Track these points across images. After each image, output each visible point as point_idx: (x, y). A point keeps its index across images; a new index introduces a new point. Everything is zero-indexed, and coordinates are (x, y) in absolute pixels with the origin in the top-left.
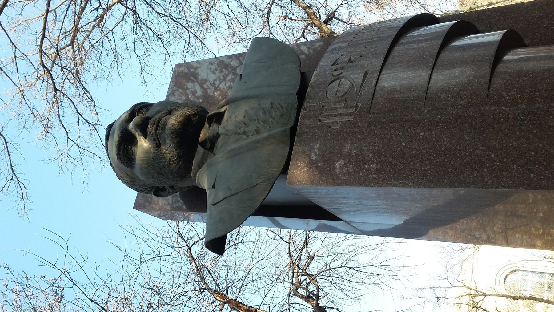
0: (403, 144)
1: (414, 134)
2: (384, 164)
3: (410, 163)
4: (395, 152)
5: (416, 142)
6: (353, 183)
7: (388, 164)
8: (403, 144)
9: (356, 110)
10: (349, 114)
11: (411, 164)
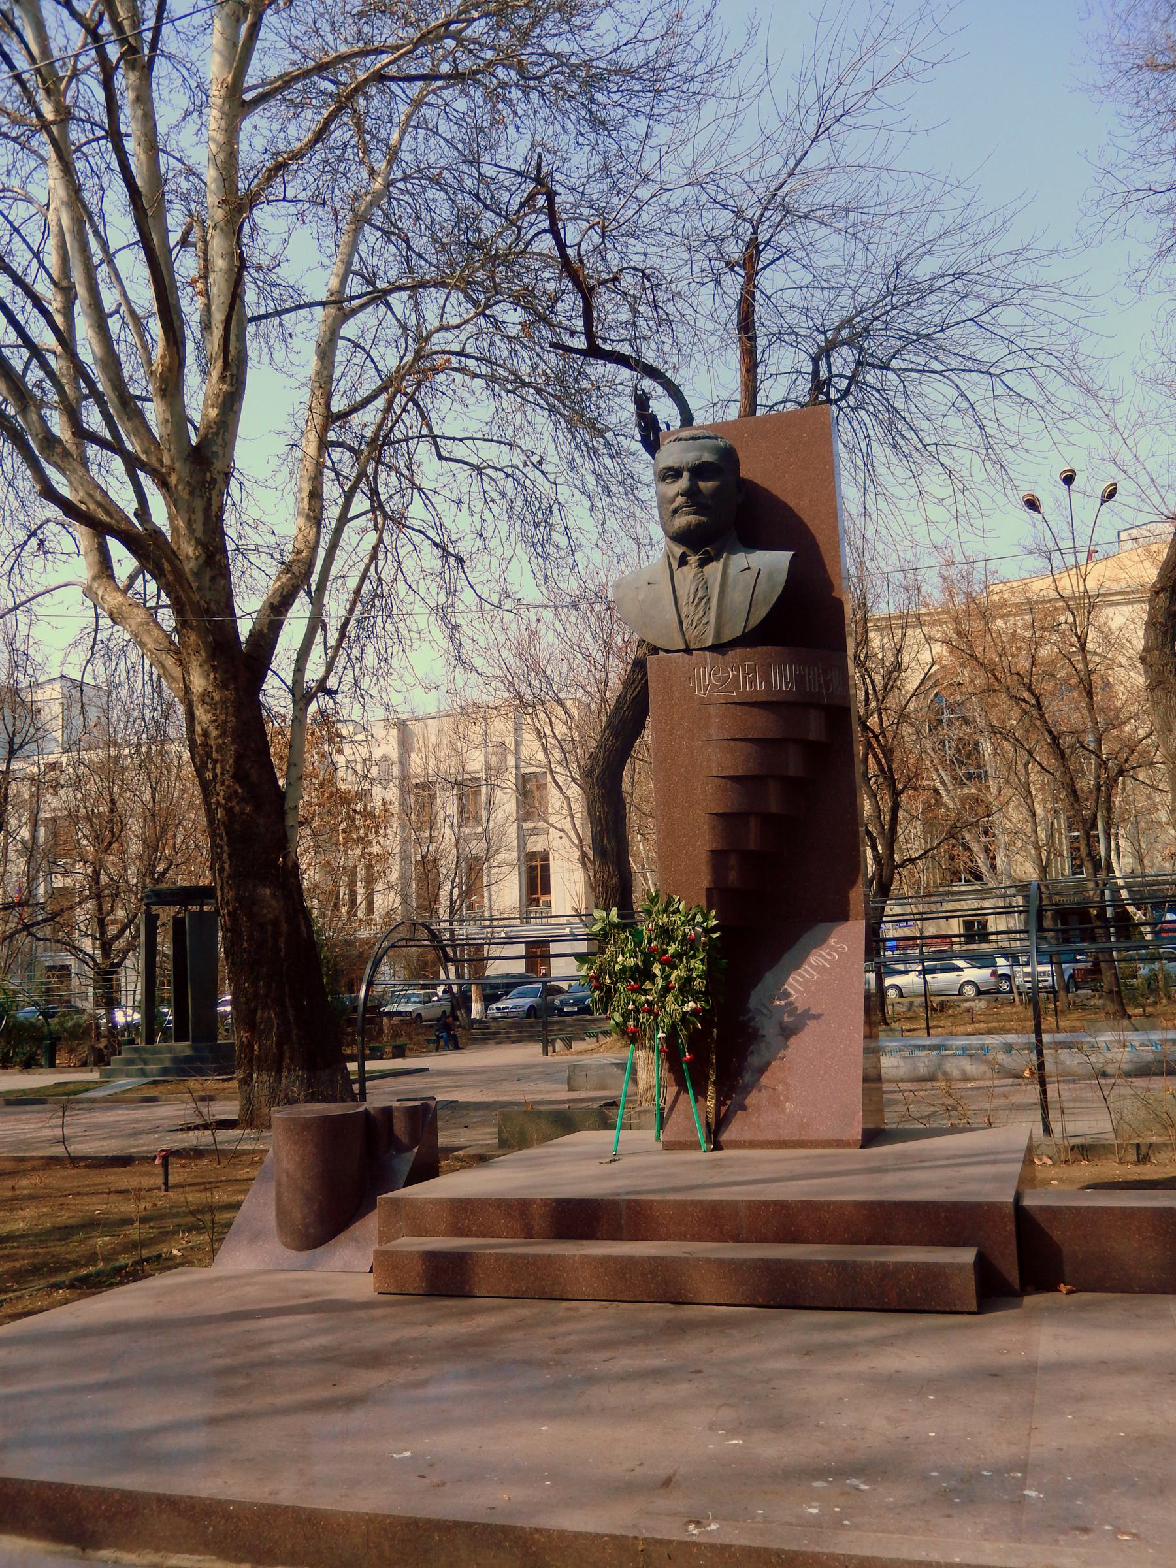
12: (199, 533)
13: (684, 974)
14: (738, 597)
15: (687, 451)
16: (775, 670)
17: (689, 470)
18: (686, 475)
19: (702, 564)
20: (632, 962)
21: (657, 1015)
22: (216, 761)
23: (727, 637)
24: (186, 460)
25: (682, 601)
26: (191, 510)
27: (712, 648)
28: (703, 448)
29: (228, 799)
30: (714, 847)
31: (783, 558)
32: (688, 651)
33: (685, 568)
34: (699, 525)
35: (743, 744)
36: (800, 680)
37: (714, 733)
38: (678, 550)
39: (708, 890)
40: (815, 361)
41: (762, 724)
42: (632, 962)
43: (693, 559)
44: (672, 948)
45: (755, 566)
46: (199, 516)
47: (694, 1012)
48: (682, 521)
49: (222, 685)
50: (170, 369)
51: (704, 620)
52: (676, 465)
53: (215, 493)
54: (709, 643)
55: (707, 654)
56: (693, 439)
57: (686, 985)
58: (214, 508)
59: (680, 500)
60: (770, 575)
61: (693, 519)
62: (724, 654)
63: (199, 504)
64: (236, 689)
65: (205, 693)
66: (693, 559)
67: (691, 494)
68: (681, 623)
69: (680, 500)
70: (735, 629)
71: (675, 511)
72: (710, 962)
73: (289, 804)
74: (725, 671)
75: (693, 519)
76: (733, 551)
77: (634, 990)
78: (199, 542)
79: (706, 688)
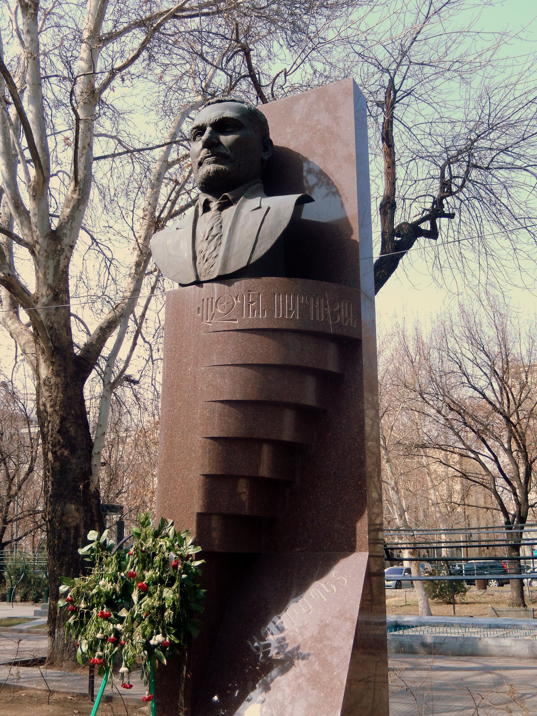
12: (50, 281)
13: (156, 604)
16: (278, 299)
17: (212, 125)
19: (221, 208)
20: (109, 586)
21: (123, 646)
22: (49, 422)
23: (232, 268)
24: (45, 237)
26: (46, 268)
27: (221, 279)
29: (54, 446)
30: (207, 472)
32: (198, 283)
34: (216, 172)
35: (243, 369)
36: (304, 310)
37: (215, 359)
39: (198, 514)
40: (443, 169)
41: (266, 351)
42: (109, 586)
43: (214, 205)
44: (148, 574)
46: (51, 271)
47: (162, 646)
49: (57, 374)
50: (38, 184)
53: (62, 258)
55: (216, 285)
57: (156, 617)
58: (61, 266)
60: (278, 212)
62: (230, 285)
63: (51, 263)
64: (65, 377)
65: (48, 379)
68: (195, 258)
72: (185, 592)
73: (95, 450)
77: (106, 617)
78: (50, 287)
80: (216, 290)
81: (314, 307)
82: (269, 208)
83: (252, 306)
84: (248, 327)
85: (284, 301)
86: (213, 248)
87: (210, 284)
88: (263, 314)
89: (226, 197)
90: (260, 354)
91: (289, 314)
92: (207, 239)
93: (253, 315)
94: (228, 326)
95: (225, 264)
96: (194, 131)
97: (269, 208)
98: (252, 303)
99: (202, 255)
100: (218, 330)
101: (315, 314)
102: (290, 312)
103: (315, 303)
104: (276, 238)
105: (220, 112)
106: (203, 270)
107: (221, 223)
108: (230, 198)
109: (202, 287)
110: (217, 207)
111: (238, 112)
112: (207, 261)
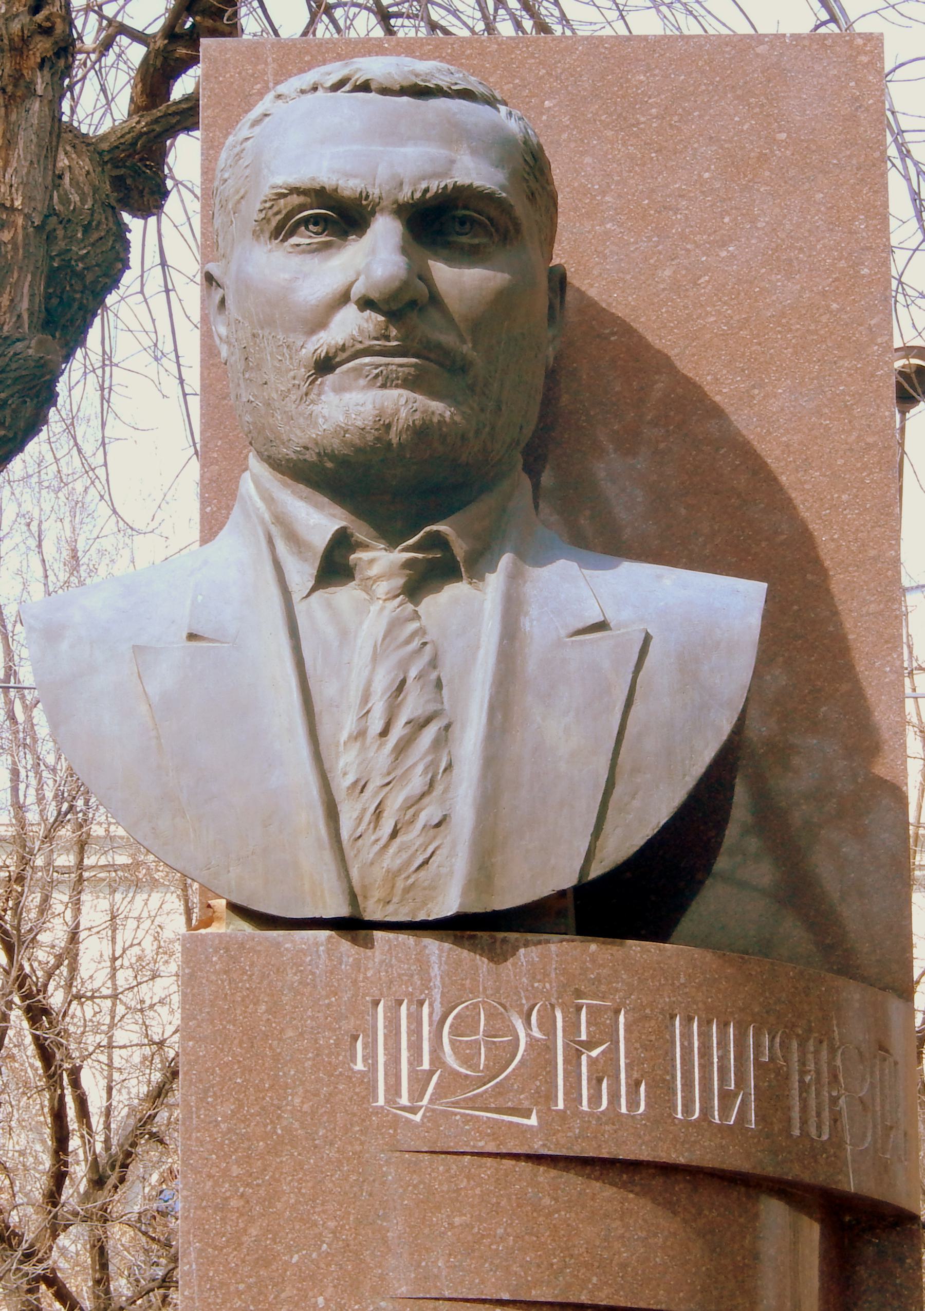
0: (295, 1258)
1: (321, 1281)
2: (242, 1215)
3: (243, 1282)
4: (274, 1240)
5: (298, 1289)
6: (189, 1139)
7: (241, 1225)
8: (295, 1258)
9: (404, 1109)
10: (394, 1089)
11: (241, 1287)
14: (567, 737)
15: (391, 134)
18: (385, 232)
25: (340, 725)
28: (454, 134)
31: (736, 603)
32: (353, 926)
33: (344, 596)
34: (423, 432)
38: (320, 521)
45: (628, 621)
48: (353, 407)
51: (429, 813)
52: (350, 186)
54: (448, 904)
55: (434, 948)
56: (420, 91)
59: (350, 324)
60: (688, 666)
61: (404, 405)
62: (498, 955)
66: (381, 561)
67: (403, 305)
69: (350, 324)
70: (552, 865)
71: (325, 365)
74: (499, 1024)
75: (404, 405)
76: (532, 554)
79: (420, 1081)
80: (435, 971)
81: (801, 1081)
82: (647, 639)
83: (592, 1062)
84: (577, 1150)
85: (705, 1052)
86: (417, 783)
87: (406, 939)
88: (633, 1103)
89: (438, 542)
90: (624, 1266)
91: (725, 1110)
92: (384, 733)
93: (595, 1099)
94: (494, 1136)
95: (483, 870)
96: (295, 200)
97: (647, 639)
98: (590, 1045)
99: (369, 800)
100: (452, 1146)
101: (804, 1109)
102: (726, 1097)
103: (802, 1063)
104: (690, 782)
105: (435, 151)
106: (378, 873)
107: (434, 663)
108: (460, 549)
109: (368, 944)
110: (400, 581)
111: (500, 164)
112: (394, 834)
